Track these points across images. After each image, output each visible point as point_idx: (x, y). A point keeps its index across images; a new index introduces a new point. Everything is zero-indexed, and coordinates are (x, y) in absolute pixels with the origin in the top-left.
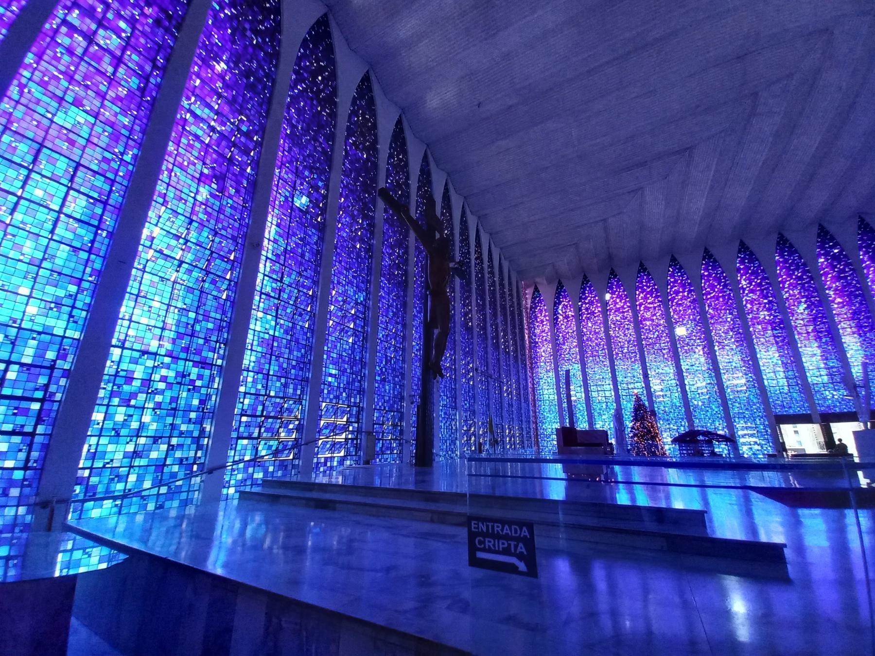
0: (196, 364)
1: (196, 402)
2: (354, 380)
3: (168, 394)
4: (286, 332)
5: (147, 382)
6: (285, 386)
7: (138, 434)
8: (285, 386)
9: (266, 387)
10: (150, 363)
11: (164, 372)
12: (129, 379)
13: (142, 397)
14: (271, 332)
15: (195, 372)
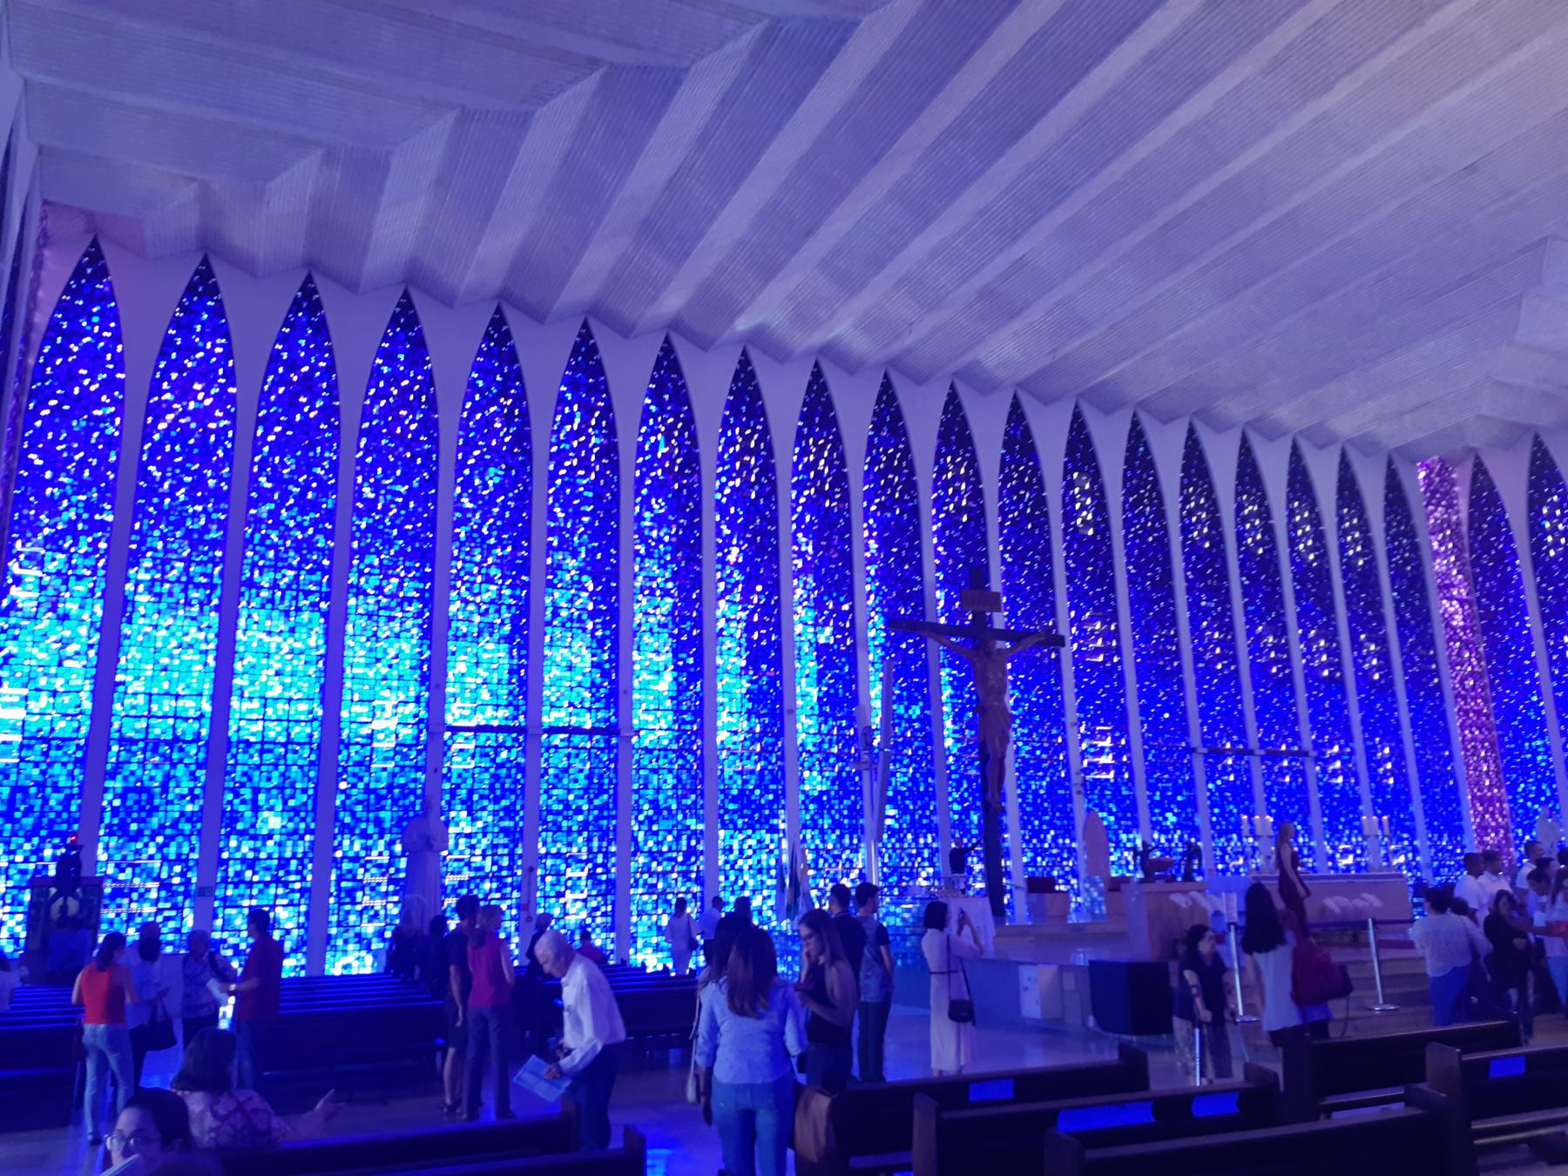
0: (768, 832)
1: (773, 862)
2: (922, 817)
3: (756, 858)
4: (833, 784)
5: (741, 851)
6: (841, 837)
7: (743, 888)
8: (841, 837)
9: (823, 841)
10: (741, 837)
11: (749, 842)
12: (731, 850)
13: (740, 862)
14: (819, 788)
15: (767, 837)
